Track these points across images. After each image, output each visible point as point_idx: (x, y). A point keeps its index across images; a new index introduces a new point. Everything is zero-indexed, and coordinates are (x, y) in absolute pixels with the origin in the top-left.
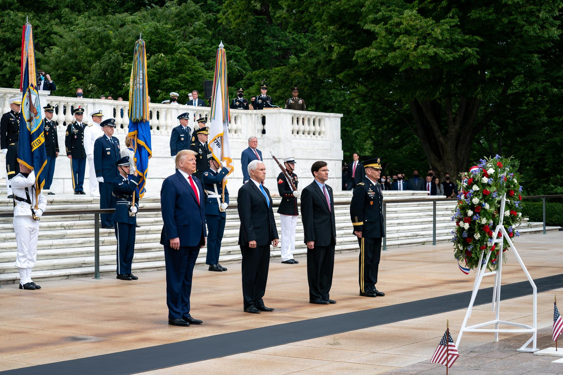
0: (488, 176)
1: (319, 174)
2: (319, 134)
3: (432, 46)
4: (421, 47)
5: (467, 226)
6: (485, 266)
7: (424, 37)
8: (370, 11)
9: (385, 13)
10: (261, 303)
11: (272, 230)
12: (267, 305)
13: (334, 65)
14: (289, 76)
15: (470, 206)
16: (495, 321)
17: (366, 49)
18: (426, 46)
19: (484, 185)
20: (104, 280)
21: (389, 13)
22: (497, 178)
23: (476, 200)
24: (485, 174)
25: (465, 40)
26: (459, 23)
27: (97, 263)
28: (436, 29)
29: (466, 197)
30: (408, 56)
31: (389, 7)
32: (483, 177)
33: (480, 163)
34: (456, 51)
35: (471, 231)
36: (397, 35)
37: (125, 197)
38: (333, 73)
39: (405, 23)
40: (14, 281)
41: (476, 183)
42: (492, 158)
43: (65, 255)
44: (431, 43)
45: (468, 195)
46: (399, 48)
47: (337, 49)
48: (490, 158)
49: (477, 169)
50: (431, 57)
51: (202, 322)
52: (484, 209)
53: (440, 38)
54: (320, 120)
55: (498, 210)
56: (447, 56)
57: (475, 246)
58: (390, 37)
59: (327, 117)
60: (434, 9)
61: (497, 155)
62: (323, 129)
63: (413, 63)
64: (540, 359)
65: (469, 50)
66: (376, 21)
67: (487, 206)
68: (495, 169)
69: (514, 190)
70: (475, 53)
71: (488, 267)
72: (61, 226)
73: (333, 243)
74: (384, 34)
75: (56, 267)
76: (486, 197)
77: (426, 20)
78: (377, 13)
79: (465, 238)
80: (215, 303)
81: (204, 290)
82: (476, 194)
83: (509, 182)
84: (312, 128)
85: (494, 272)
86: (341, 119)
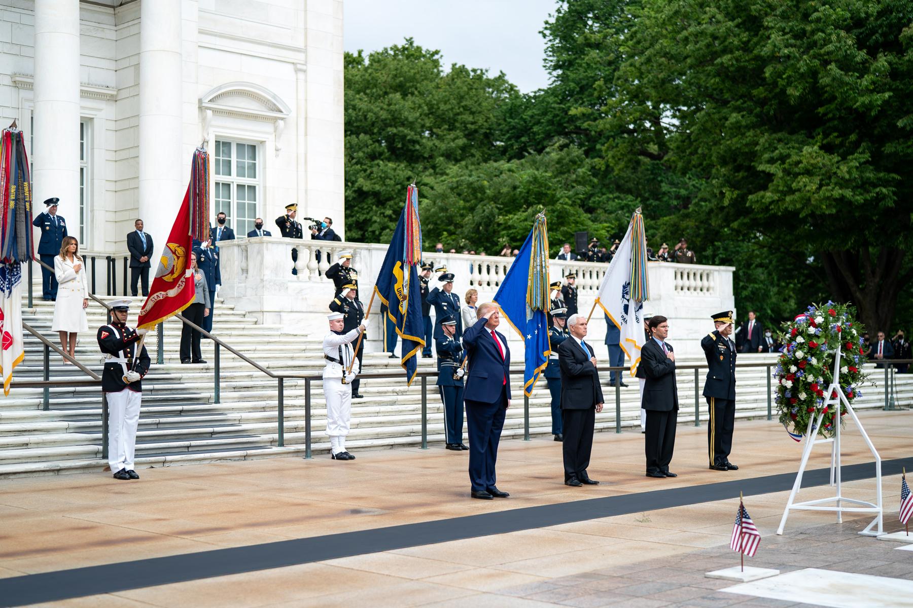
0: (815, 326)
1: (657, 330)
2: (708, 290)
3: (837, 188)
4: (824, 188)
5: (789, 384)
6: (816, 431)
7: (828, 177)
8: (765, 150)
9: (782, 151)
10: (585, 475)
11: (597, 393)
12: (591, 477)
13: (728, 213)
14: (678, 226)
15: (793, 361)
16: (837, 498)
17: (762, 193)
18: (830, 188)
19: (810, 336)
20: (431, 450)
21: (787, 151)
22: (827, 328)
23: (800, 354)
24: (812, 324)
25: (879, 179)
26: (870, 159)
27: (424, 432)
28: (842, 167)
29: (789, 351)
30: (809, 200)
31: (787, 144)
32: (809, 326)
33: (808, 310)
34: (868, 192)
35: (795, 390)
36: (796, 175)
37: (451, 358)
38: (727, 222)
39: (805, 161)
40: (329, 451)
41: (801, 334)
42: (823, 305)
43: (392, 423)
44: (836, 184)
45: (791, 348)
46: (799, 190)
47: (730, 195)
48: (820, 305)
49: (804, 318)
50: (835, 200)
51: (508, 495)
52: (811, 365)
53: (847, 177)
54: (708, 275)
55: (832, 367)
56: (858, 198)
57: (800, 409)
58: (788, 178)
59: (716, 271)
60: (842, 144)
61: (830, 302)
62: (712, 284)
63: (817, 207)
64: (883, 545)
65: (884, 190)
66: (771, 161)
67: (814, 361)
68: (825, 318)
69: (852, 342)
70: (891, 194)
71: (820, 433)
72: (393, 392)
73: (676, 408)
74: (780, 174)
75: (380, 436)
76: (813, 350)
77: (830, 157)
78: (773, 151)
79: (788, 399)
80: (537, 475)
81: (535, 462)
82: (800, 347)
83: (845, 333)
84: (699, 283)
85: (831, 440)
86: (734, 273)
